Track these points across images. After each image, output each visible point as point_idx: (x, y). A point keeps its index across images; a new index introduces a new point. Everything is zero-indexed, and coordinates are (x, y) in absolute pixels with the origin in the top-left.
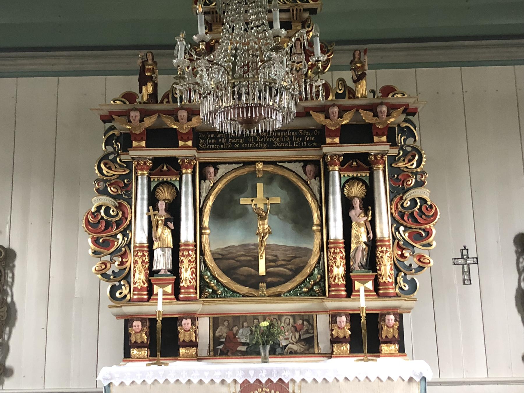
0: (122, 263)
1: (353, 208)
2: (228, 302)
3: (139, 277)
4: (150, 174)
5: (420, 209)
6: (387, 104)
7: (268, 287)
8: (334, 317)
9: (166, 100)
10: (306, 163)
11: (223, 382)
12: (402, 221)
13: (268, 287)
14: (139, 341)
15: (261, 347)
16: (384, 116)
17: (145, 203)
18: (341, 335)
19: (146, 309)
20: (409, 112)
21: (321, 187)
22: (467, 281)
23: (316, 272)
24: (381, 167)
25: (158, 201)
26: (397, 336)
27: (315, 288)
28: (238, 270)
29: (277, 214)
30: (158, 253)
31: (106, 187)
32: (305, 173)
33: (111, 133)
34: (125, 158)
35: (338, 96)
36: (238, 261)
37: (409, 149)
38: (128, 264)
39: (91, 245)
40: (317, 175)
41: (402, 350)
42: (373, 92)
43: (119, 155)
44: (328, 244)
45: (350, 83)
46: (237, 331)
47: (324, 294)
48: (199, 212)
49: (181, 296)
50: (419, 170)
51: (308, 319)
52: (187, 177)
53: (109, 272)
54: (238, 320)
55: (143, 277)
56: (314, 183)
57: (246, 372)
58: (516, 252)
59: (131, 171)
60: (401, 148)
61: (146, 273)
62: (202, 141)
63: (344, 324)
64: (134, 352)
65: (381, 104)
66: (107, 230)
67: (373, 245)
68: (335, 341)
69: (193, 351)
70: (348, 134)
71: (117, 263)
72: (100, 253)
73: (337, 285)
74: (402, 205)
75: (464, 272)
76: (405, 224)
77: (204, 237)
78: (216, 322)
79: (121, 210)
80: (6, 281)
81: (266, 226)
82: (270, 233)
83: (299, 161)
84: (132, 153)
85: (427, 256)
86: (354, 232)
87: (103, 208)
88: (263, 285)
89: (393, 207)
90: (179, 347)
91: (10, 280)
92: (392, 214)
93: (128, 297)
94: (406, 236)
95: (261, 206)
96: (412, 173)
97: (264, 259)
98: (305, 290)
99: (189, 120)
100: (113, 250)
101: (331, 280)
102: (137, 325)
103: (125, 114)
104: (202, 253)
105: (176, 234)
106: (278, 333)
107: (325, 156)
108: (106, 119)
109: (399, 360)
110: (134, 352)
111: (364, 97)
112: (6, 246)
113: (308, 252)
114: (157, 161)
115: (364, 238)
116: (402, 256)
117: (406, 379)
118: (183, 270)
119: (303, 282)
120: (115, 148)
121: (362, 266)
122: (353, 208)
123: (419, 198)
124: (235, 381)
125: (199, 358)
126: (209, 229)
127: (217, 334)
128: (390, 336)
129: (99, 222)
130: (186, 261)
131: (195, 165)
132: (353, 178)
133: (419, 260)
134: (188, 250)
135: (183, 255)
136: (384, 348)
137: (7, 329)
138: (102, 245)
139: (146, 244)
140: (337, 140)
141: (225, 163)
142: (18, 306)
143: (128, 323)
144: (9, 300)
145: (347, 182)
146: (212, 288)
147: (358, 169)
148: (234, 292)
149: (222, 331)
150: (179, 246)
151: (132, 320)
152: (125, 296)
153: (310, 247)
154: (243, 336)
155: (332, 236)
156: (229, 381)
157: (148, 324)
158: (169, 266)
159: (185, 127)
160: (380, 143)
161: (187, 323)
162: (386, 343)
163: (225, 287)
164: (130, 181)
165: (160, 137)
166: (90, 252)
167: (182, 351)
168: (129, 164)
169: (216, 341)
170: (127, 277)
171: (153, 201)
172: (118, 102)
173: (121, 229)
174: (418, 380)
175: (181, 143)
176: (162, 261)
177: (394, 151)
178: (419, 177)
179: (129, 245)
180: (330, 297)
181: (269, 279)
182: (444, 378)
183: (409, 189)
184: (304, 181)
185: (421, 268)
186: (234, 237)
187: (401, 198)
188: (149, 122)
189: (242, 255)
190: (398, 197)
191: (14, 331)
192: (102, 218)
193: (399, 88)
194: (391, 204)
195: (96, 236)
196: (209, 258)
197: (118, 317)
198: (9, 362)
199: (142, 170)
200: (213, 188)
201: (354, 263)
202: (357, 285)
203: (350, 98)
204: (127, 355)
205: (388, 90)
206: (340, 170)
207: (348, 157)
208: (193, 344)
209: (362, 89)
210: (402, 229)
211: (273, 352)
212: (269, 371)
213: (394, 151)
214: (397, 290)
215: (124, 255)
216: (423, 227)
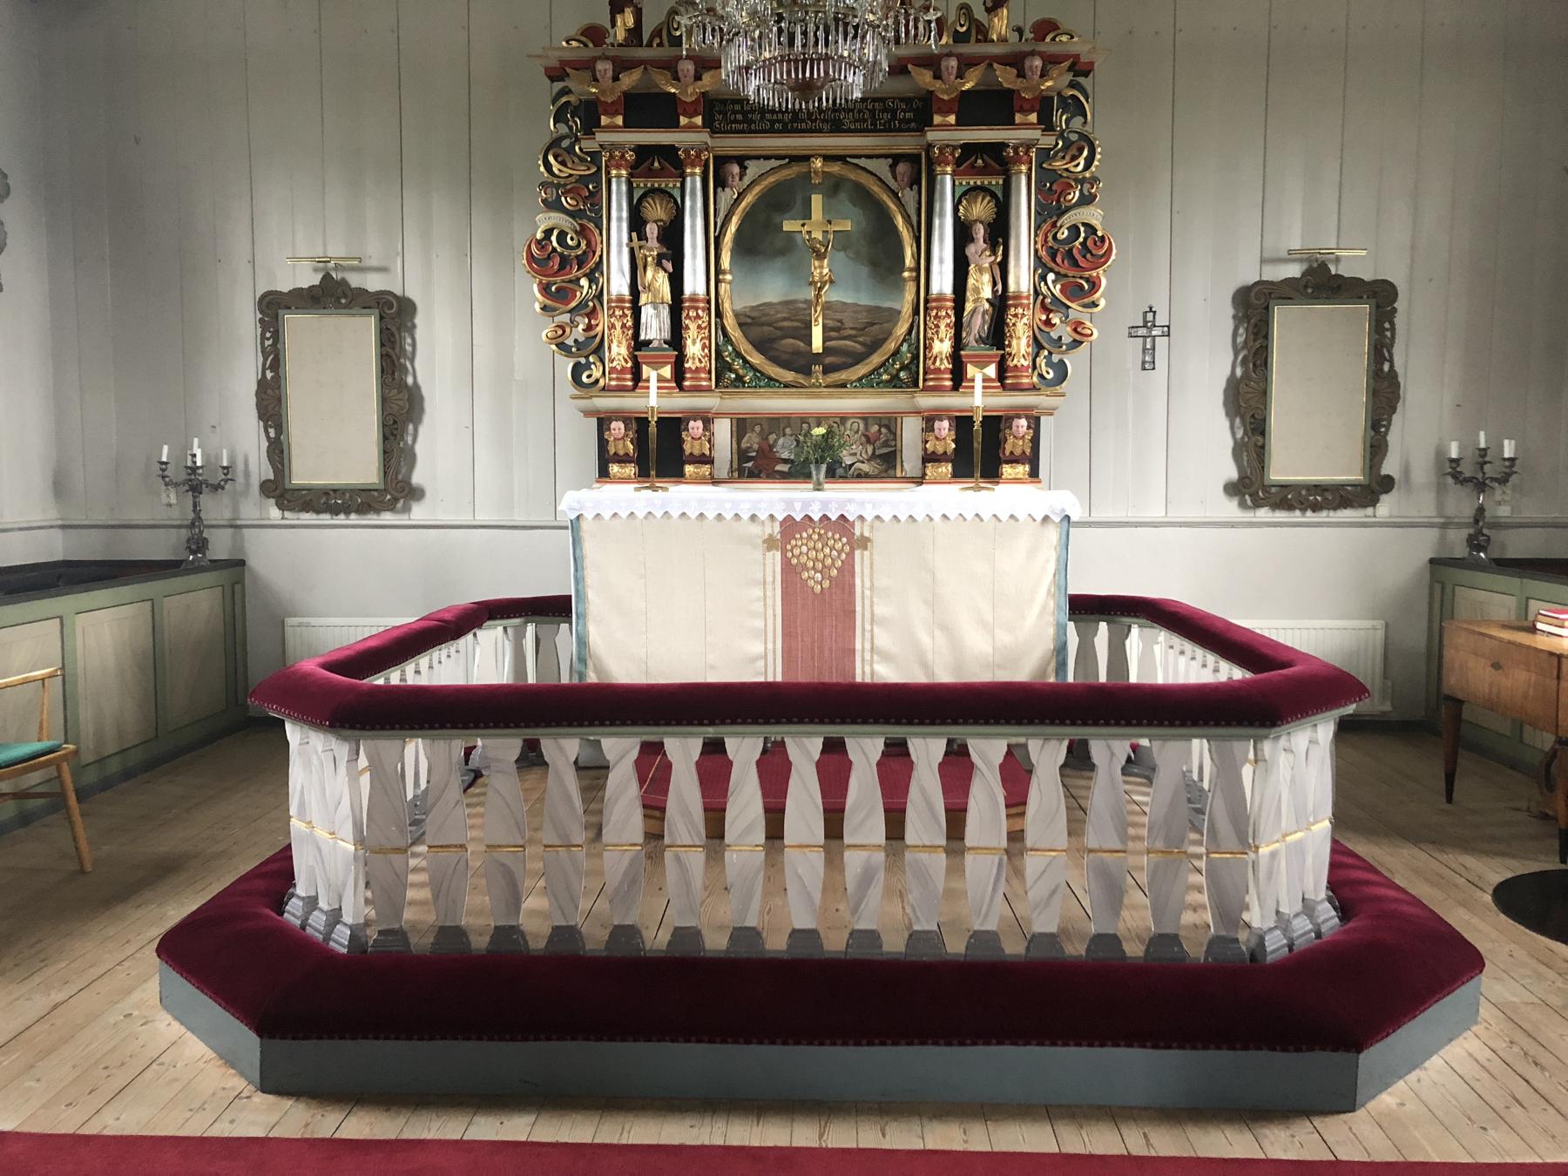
0: (589, 328)
1: (972, 240)
2: (761, 396)
3: (618, 351)
4: (631, 175)
5: (1084, 244)
6: (1041, 55)
7: (825, 372)
8: (930, 421)
9: (657, 41)
10: (896, 159)
11: (753, 518)
12: (1053, 265)
13: (825, 372)
14: (621, 453)
15: (813, 467)
16: (1036, 77)
17: (625, 225)
18: (940, 450)
20: (1080, 69)
21: (919, 203)
22: (1148, 365)
23: (905, 348)
24: (1024, 168)
25: (645, 223)
26: (1028, 451)
27: (902, 374)
28: (777, 341)
29: (844, 249)
30: (647, 313)
31: (559, 197)
32: (895, 178)
33: (564, 100)
34: (589, 145)
35: (959, 38)
36: (780, 329)
37: (1074, 137)
38: (599, 329)
39: (538, 295)
40: (915, 181)
41: (1034, 473)
42: (1020, 31)
43: (577, 140)
44: (927, 301)
45: (980, 14)
46: (776, 441)
47: (916, 385)
48: (713, 244)
49: (687, 383)
50: (1087, 175)
51: (889, 423)
52: (694, 182)
53: (570, 342)
54: (777, 423)
55: (624, 351)
56: (909, 196)
57: (789, 503)
58: (1234, 317)
59: (599, 169)
60: (1061, 136)
61: (628, 347)
62: (717, 117)
63: (945, 432)
64: (614, 469)
65: (1033, 53)
66: (563, 269)
67: (1001, 303)
68: (929, 458)
69: (705, 469)
71: (581, 327)
72: (555, 309)
73: (938, 370)
74: (1055, 237)
75: (1144, 350)
76: (1057, 269)
77: (723, 287)
78: (741, 426)
79: (585, 237)
80: (403, 350)
81: (826, 271)
82: (832, 282)
83: (886, 156)
84: (602, 137)
85: (1088, 324)
86: (971, 282)
87: (555, 232)
88: (818, 368)
89: (1039, 239)
90: (684, 463)
91: (409, 348)
92: (1036, 251)
93: (602, 383)
94: (1057, 290)
95: (818, 235)
96: (1076, 180)
97: (820, 328)
98: (885, 377)
99: (698, 78)
100: (573, 304)
101: (929, 362)
102: (618, 427)
103: (587, 66)
104: (719, 315)
105: (676, 280)
106: (841, 446)
107: (929, 147)
108: (555, 74)
109: (1029, 489)
110: (614, 469)
111: (1003, 40)
112: (398, 292)
113: (894, 315)
114: (643, 152)
115: (987, 293)
116: (1048, 322)
117: (1039, 518)
118: (689, 342)
119: (883, 365)
120: (571, 128)
121: (980, 340)
122: (972, 240)
123: (1084, 224)
124: (772, 516)
125: (715, 481)
126: (731, 272)
127: (744, 445)
128: (1018, 452)
129: (549, 257)
130: (693, 326)
131: (707, 161)
132: (976, 188)
133: (1075, 330)
134: (696, 309)
135: (688, 317)
136: (1007, 470)
137: (411, 427)
138: (556, 296)
139: (628, 297)
140: (952, 119)
141: (758, 158)
142: (425, 392)
143: (603, 423)
144: (410, 380)
145: (965, 194)
146: (735, 372)
147: (984, 171)
148: (771, 379)
150: (682, 302)
151: (610, 420)
152: (597, 381)
153: (897, 306)
154: (785, 448)
155: (935, 289)
156: (763, 516)
157: (634, 426)
158: (666, 335)
159: (690, 92)
160: (1027, 126)
161: (696, 426)
162: (1007, 462)
163: (755, 370)
164: (598, 187)
165: (648, 108)
166: (537, 307)
167: (689, 469)
168: (595, 156)
169: (742, 455)
170: (599, 350)
171: (637, 224)
172: (574, 43)
173: (586, 269)
174: (1057, 520)
175: (683, 120)
176: (655, 325)
177: (1047, 141)
178: (1086, 186)
179: (599, 296)
180: (925, 389)
181: (829, 360)
182: (1096, 517)
183: (1068, 209)
184: (892, 191)
185: (1076, 343)
186: (771, 289)
187: (1054, 225)
188: (629, 80)
189: (785, 319)
190: (1050, 222)
191: (421, 430)
192: (554, 250)
193: (1065, 24)
194: (1036, 235)
195: (545, 280)
196: (730, 322)
197: (588, 413)
198: (417, 478)
199: (618, 167)
200: (737, 202)
201: (968, 334)
202: (971, 370)
203: (978, 41)
204: (604, 473)
205: (1046, 28)
206: (954, 174)
207: (970, 149)
208: (706, 460)
209: (1000, 24)
210: (1051, 277)
211: (832, 474)
212: (825, 504)
213: (1047, 141)
214: (1035, 379)
215: (592, 314)
216: (1087, 274)
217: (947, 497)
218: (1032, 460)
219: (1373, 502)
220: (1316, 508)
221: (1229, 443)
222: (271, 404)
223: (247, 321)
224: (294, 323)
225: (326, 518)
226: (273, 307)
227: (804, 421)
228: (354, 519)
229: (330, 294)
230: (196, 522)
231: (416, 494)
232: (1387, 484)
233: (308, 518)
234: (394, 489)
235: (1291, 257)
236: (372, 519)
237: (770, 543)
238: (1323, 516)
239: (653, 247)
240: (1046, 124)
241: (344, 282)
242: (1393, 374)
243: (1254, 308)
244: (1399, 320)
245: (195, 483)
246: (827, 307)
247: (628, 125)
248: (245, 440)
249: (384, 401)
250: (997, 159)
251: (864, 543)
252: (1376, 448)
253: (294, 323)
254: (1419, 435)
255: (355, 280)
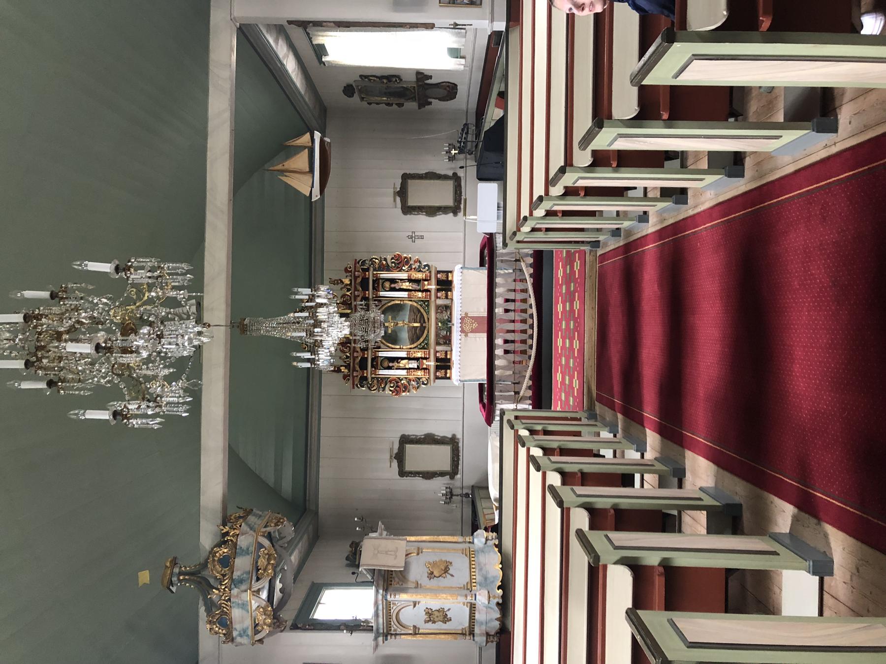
3: (420, 373)
8: (437, 297)
19: (432, 370)
20: (356, 262)
22: (422, 237)
28: (417, 335)
30: (411, 366)
34: (370, 380)
41: (451, 272)
51: (438, 307)
54: (437, 335)
56: (383, 303)
66: (399, 387)
67: (410, 280)
70: (365, 287)
78: (438, 344)
84: (369, 376)
109: (455, 273)
111: (351, 280)
114: (372, 366)
115: (407, 284)
138: (406, 388)
143: (437, 378)
149: (441, 341)
161: (438, 355)
165: (363, 364)
168: (372, 378)
169: (445, 343)
170: (419, 379)
171: (390, 368)
176: (414, 364)
177: (371, 269)
185: (420, 262)
186: (405, 335)
188: (358, 368)
196: (412, 346)
202: (426, 288)
204: (449, 378)
205: (346, 270)
207: (374, 288)
208: (446, 352)
209: (347, 281)
211: (450, 321)
213: (371, 269)
217: (456, 294)
218: (447, 272)
219: (459, 178)
220: (461, 193)
221: (443, 216)
222: (429, 475)
223: (408, 481)
224: (408, 468)
225: (460, 462)
226: (403, 473)
227: (437, 327)
228: (461, 454)
229: (400, 457)
230: (461, 495)
231: (454, 436)
232: (455, 174)
233: (460, 467)
234: (453, 442)
235: (395, 200)
236: (461, 449)
237: (466, 336)
238: (463, 191)
239: (395, 364)
240: (368, 270)
241: (396, 454)
242: (426, 174)
243: (408, 210)
244: (412, 172)
245: (450, 495)
246: (409, 322)
247: (366, 369)
248: (439, 485)
249: (428, 443)
250: (377, 281)
251: (466, 314)
252: (445, 177)
253: (408, 468)
254: (443, 166)
255: (396, 451)
